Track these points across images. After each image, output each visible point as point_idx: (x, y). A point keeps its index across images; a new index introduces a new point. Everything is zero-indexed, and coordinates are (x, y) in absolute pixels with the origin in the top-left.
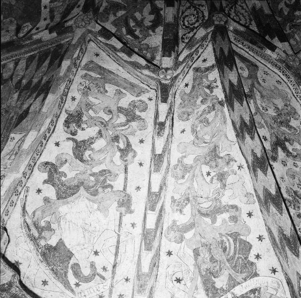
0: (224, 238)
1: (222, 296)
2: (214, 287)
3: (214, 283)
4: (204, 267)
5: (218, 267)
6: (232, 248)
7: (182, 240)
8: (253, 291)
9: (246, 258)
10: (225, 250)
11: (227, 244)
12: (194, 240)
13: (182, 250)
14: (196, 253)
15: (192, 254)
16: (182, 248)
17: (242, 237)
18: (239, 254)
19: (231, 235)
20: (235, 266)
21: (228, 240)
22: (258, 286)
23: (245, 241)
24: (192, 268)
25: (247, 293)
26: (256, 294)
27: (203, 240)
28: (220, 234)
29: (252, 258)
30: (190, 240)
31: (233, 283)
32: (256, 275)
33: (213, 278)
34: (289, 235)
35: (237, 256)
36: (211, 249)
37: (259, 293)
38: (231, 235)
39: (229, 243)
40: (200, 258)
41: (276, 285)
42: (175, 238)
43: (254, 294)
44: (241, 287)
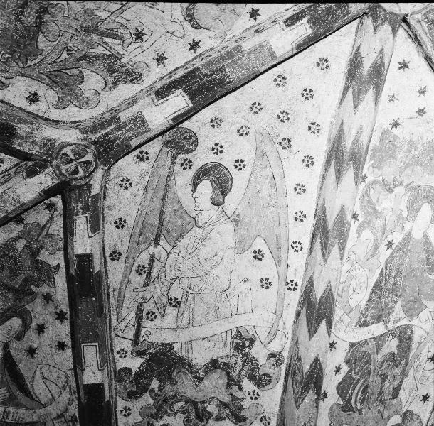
0: (359, 405)
1: (397, 327)
2: (401, 341)
3: (398, 346)
4: (397, 371)
5: (384, 367)
6: (356, 390)
7: (405, 414)
8: (365, 324)
9: (350, 371)
10: (365, 390)
11: (359, 396)
12: (391, 412)
13: (409, 400)
14: (396, 394)
15: (401, 392)
16: (408, 403)
17: (342, 403)
18: (354, 379)
19: (351, 409)
20: (366, 363)
21: (356, 402)
22: (356, 330)
23: (340, 396)
24: (411, 372)
25: (373, 323)
26: (363, 319)
27: (382, 409)
28: (360, 413)
29: (345, 369)
30: (396, 412)
31: (379, 341)
32: (352, 345)
33: (396, 353)
34: (311, 391)
35: (358, 377)
36: (379, 394)
37: (359, 321)
38: (351, 409)
39: (357, 397)
40: (395, 384)
41: (339, 326)
42: (411, 419)
43: (365, 321)
44: (375, 333)
